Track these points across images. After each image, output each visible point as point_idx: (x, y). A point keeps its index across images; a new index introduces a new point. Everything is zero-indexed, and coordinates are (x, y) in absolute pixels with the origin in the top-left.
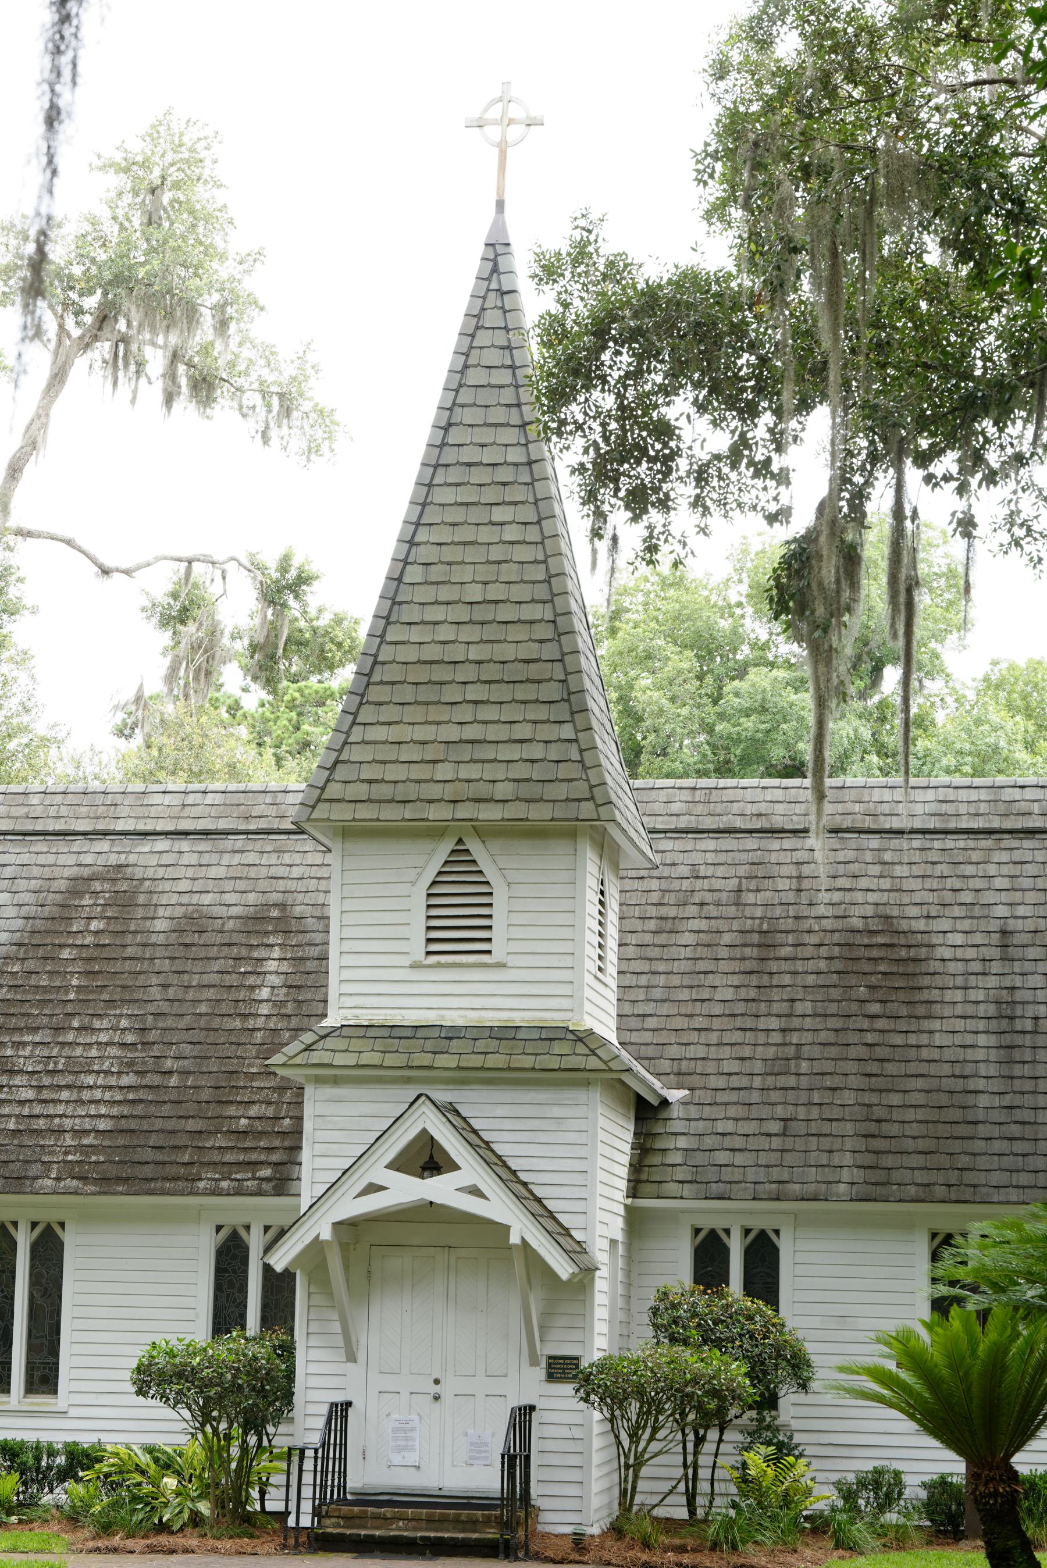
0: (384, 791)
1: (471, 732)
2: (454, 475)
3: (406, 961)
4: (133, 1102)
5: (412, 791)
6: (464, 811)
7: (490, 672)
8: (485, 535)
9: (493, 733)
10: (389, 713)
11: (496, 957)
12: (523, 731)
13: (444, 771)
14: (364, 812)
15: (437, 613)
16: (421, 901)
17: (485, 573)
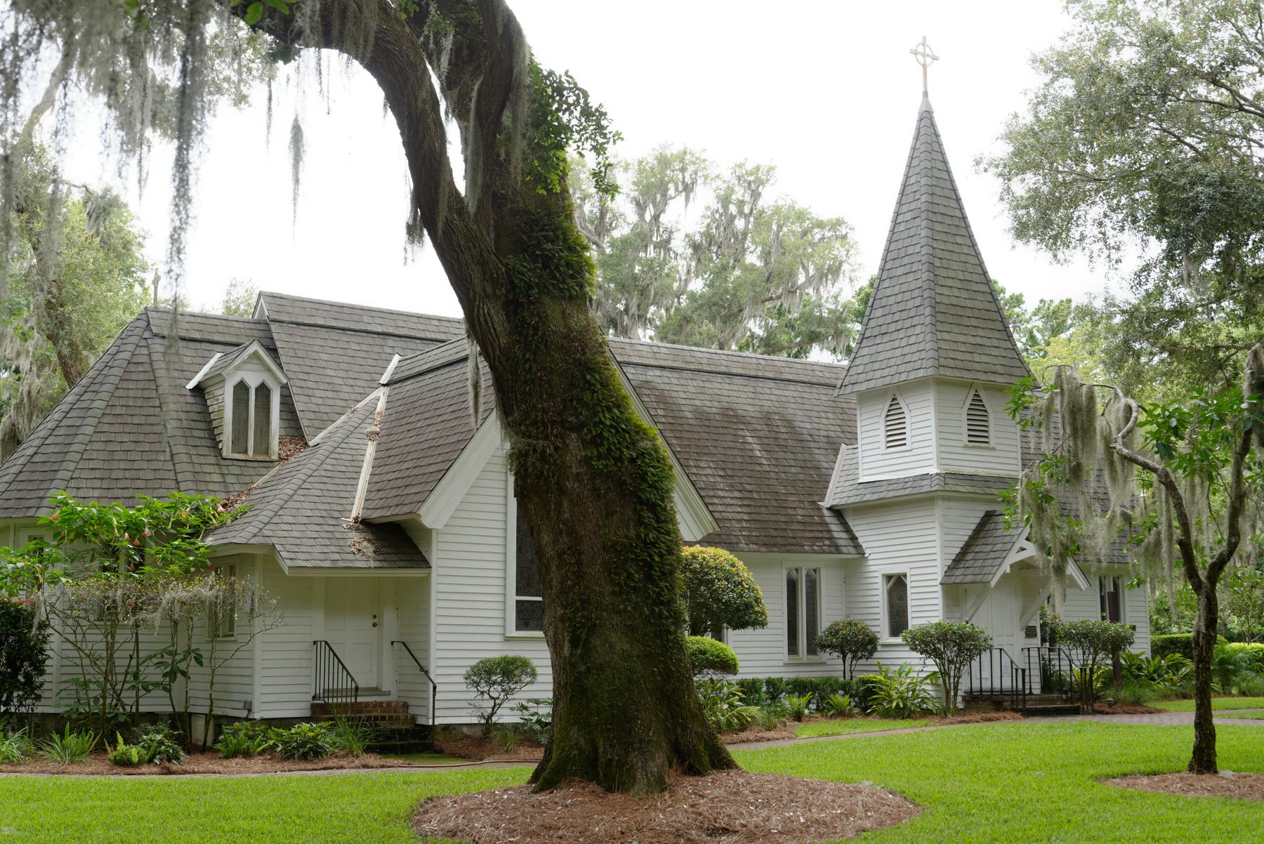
0: (959, 364)
1: (979, 340)
2: (939, 218)
3: (961, 444)
4: (748, 506)
5: (971, 366)
6: (991, 377)
7: (976, 314)
8: (956, 248)
9: (986, 342)
10: (947, 327)
11: (992, 444)
12: (996, 343)
13: (977, 358)
14: (957, 373)
15: (950, 283)
16: (965, 417)
17: (961, 266)
